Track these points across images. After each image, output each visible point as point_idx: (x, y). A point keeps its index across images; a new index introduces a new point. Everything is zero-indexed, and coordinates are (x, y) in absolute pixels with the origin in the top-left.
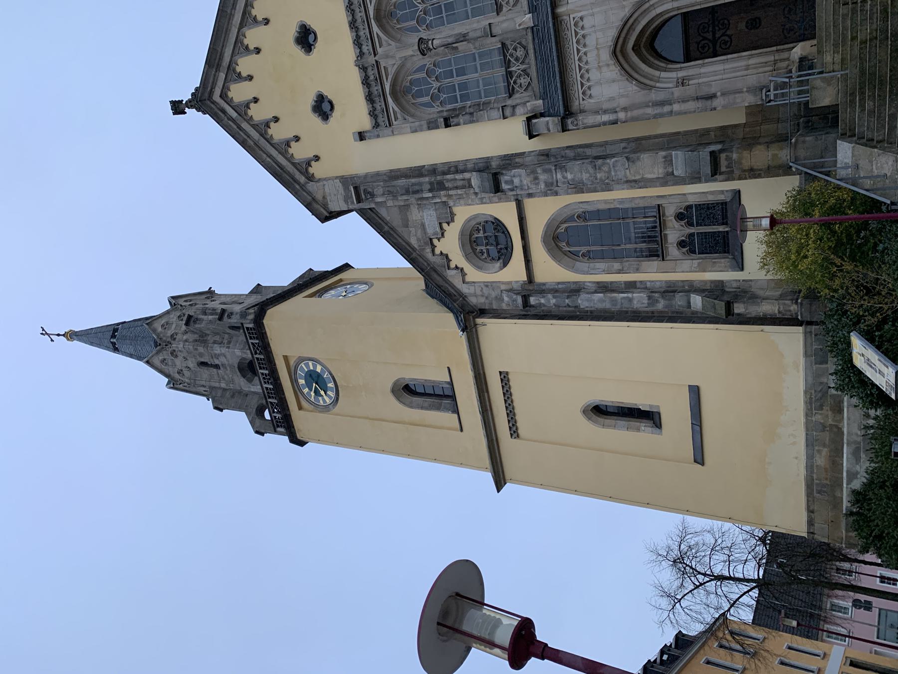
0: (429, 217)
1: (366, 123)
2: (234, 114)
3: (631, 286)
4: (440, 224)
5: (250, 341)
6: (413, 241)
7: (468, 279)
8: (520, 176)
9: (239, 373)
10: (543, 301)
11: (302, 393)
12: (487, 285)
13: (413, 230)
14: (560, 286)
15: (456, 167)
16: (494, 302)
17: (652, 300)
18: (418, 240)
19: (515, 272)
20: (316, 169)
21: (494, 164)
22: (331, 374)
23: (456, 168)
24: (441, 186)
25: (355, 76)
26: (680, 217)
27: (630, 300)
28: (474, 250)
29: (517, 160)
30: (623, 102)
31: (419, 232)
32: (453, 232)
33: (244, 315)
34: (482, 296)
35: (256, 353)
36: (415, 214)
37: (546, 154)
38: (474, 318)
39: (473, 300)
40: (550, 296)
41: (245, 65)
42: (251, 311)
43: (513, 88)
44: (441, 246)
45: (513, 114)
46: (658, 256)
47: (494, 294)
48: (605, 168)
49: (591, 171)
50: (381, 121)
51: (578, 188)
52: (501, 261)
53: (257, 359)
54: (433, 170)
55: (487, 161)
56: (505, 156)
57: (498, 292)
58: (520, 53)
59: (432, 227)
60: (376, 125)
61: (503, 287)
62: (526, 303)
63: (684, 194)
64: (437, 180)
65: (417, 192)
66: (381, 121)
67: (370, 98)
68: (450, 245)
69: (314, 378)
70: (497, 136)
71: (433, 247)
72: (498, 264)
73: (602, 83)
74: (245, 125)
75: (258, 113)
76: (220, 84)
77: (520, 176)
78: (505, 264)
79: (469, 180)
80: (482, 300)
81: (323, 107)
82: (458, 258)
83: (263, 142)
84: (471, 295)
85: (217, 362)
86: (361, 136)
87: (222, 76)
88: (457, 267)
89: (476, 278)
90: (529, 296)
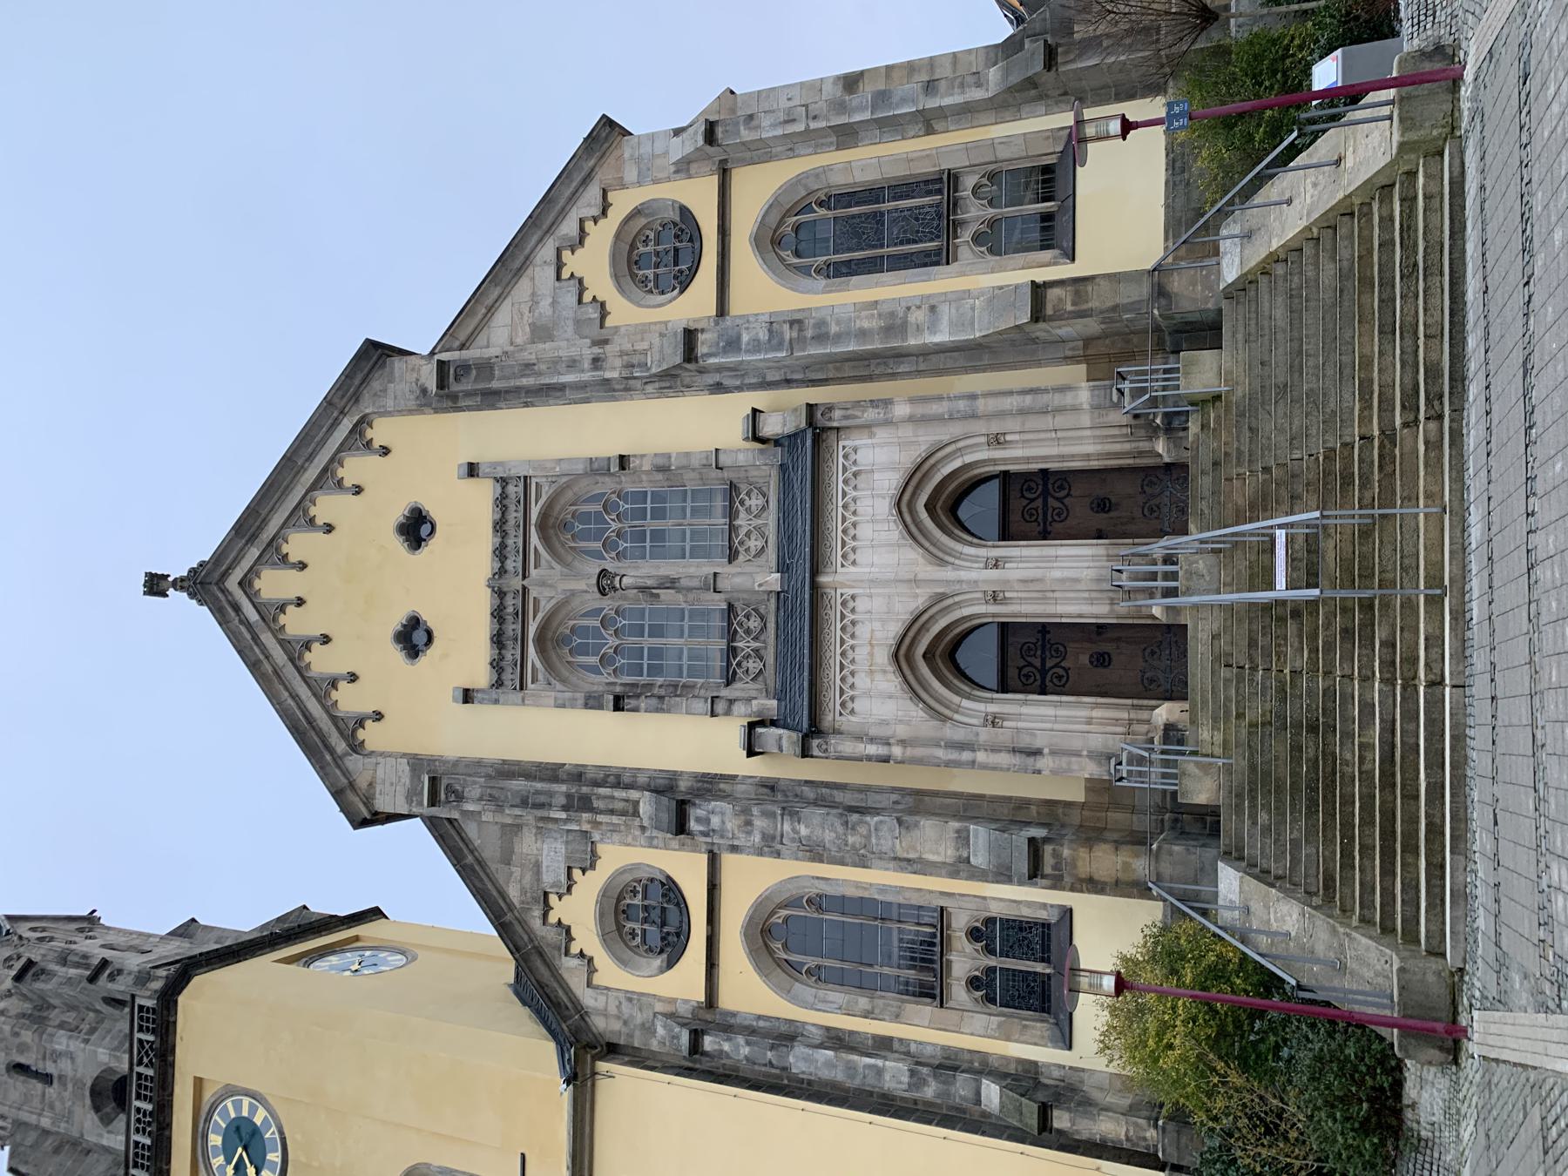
0: (552, 854)
1: (481, 676)
2: (253, 616)
3: (884, 1045)
4: (569, 868)
5: (137, 1035)
6: (514, 893)
7: (598, 979)
8: (723, 814)
9: (88, 1101)
10: (726, 1047)
11: (208, 1166)
12: (630, 997)
13: (517, 871)
14: (761, 1023)
15: (618, 776)
16: (637, 1033)
17: (917, 1081)
18: (523, 891)
19: (683, 982)
20: (371, 735)
21: (683, 785)
22: (281, 1133)
23: (617, 779)
24: (585, 804)
25: (481, 603)
26: (974, 934)
27: (879, 1072)
28: (620, 927)
29: (722, 786)
30: (901, 731)
31: (528, 877)
32: (590, 887)
33: (143, 978)
34: (618, 1018)
35: (140, 1063)
36: (527, 844)
37: (770, 786)
38: (595, 1058)
39: (599, 1023)
40: (741, 1040)
41: (298, 544)
42: (162, 972)
43: (735, 672)
44: (561, 910)
45: (728, 713)
46: (933, 997)
47: (639, 1018)
48: (863, 830)
49: (840, 829)
50: (507, 676)
51: (815, 853)
52: (665, 956)
53: (139, 1075)
54: (578, 775)
55: (673, 776)
56: (704, 775)
58: (754, 624)
59: (553, 873)
60: (499, 684)
61: (659, 1007)
62: (695, 1047)
63: (984, 898)
64: (581, 792)
65: (541, 806)
66: (507, 676)
67: (498, 640)
68: (579, 911)
69: (245, 1136)
70: (695, 741)
71: (547, 908)
72: (658, 962)
73: (872, 696)
74: (267, 638)
75: (295, 623)
76: (246, 564)
77: (723, 814)
78: (670, 965)
79: (636, 803)
80: (616, 1026)
81: (413, 638)
82: (587, 938)
83: (290, 672)
85: (50, 1068)
86: (467, 696)
87: (254, 552)
88: (582, 954)
89: (615, 983)
90: (703, 1032)
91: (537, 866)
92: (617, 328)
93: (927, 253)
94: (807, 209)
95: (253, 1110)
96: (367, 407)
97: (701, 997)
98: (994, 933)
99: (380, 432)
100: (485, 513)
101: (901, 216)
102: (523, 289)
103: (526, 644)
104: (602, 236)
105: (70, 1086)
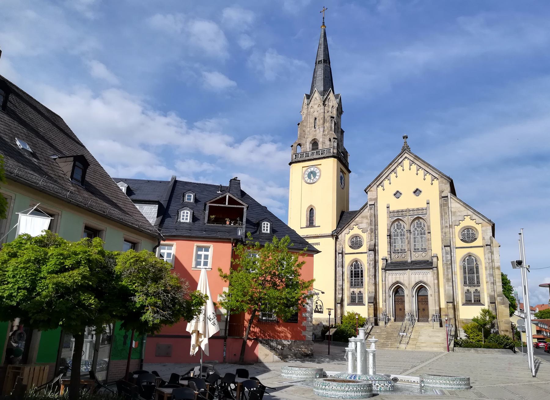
1: (391, 209)
2: (400, 161)
24: (372, 232)
25: (404, 208)
36: (365, 221)
41: (414, 167)
44: (355, 227)
58: (403, 256)
59: (362, 226)
67: (398, 212)
70: (383, 251)
73: (393, 277)
74: (396, 165)
76: (410, 158)
83: (390, 171)
87: (412, 159)
91: (362, 223)
94: (476, 261)
95: (318, 173)
96: (440, 179)
98: (361, 295)
99: (436, 182)
100: (420, 207)
101: (473, 277)
102: (463, 209)
103: (397, 218)
104: (472, 224)
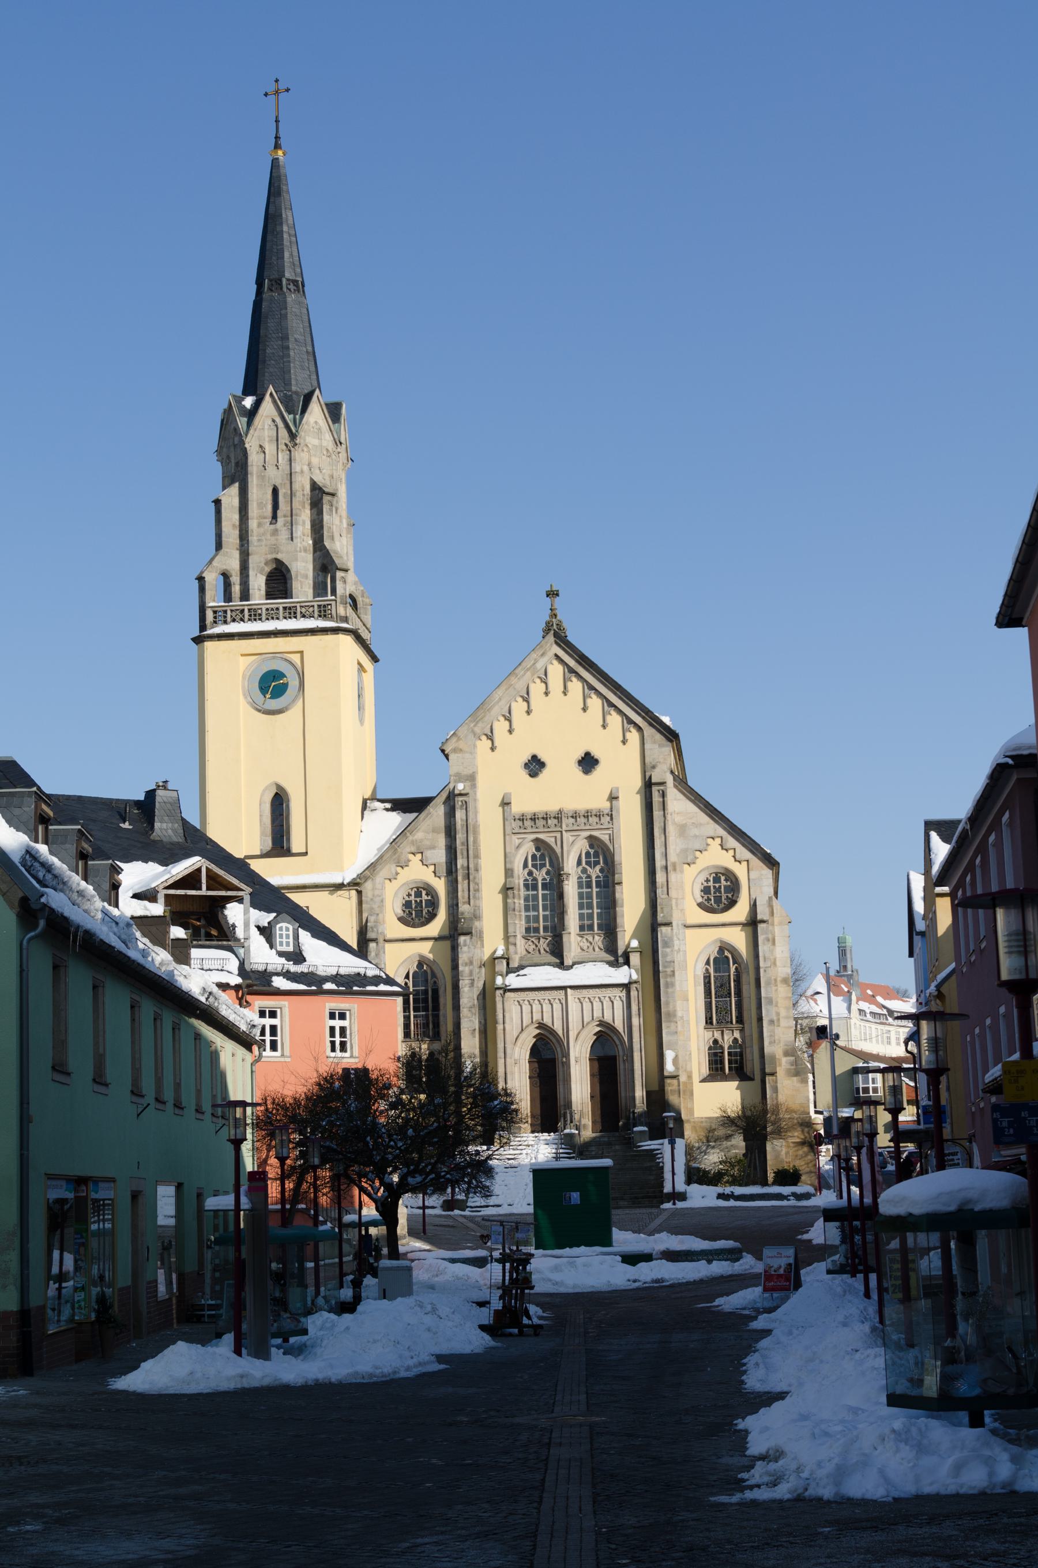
1: (517, 808)
13: (430, 836)
18: (421, 841)
31: (428, 843)
47: (375, 906)
57: (377, 911)
78: (400, 919)
84: (374, 884)
85: (281, 520)
88: (397, 874)
92: (682, 871)
93: (711, 1018)
97: (389, 936)
105: (273, 538)
